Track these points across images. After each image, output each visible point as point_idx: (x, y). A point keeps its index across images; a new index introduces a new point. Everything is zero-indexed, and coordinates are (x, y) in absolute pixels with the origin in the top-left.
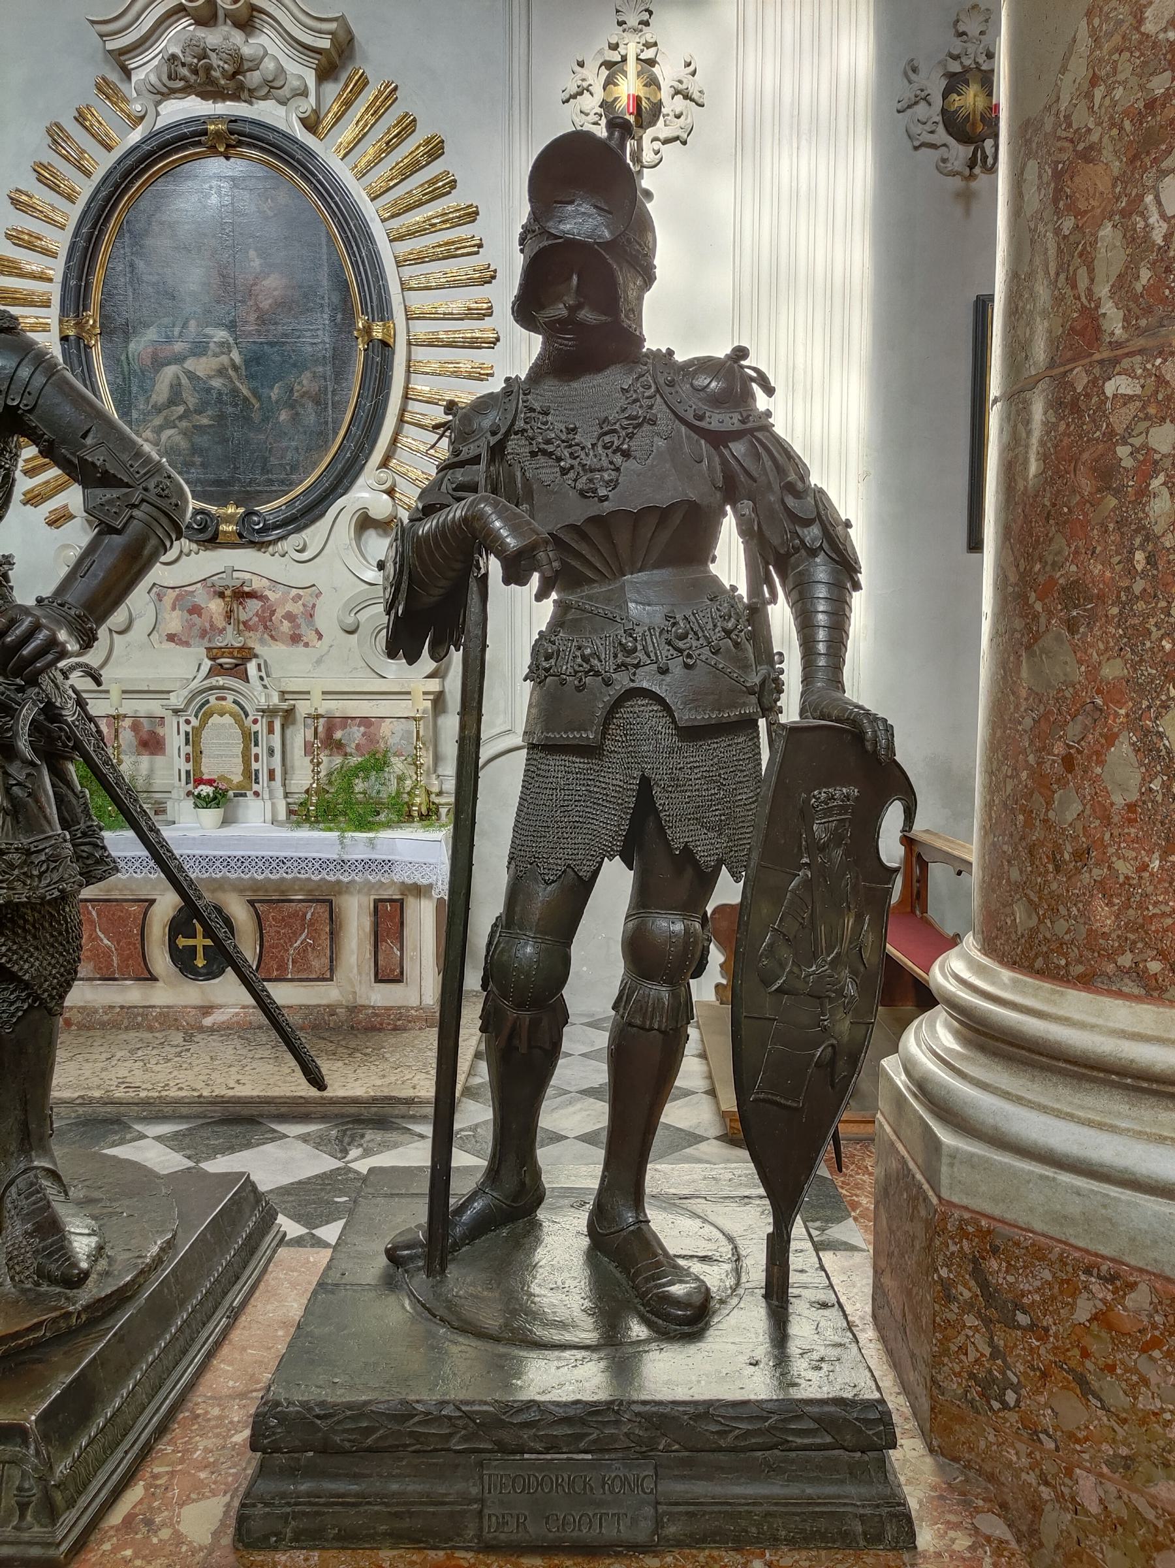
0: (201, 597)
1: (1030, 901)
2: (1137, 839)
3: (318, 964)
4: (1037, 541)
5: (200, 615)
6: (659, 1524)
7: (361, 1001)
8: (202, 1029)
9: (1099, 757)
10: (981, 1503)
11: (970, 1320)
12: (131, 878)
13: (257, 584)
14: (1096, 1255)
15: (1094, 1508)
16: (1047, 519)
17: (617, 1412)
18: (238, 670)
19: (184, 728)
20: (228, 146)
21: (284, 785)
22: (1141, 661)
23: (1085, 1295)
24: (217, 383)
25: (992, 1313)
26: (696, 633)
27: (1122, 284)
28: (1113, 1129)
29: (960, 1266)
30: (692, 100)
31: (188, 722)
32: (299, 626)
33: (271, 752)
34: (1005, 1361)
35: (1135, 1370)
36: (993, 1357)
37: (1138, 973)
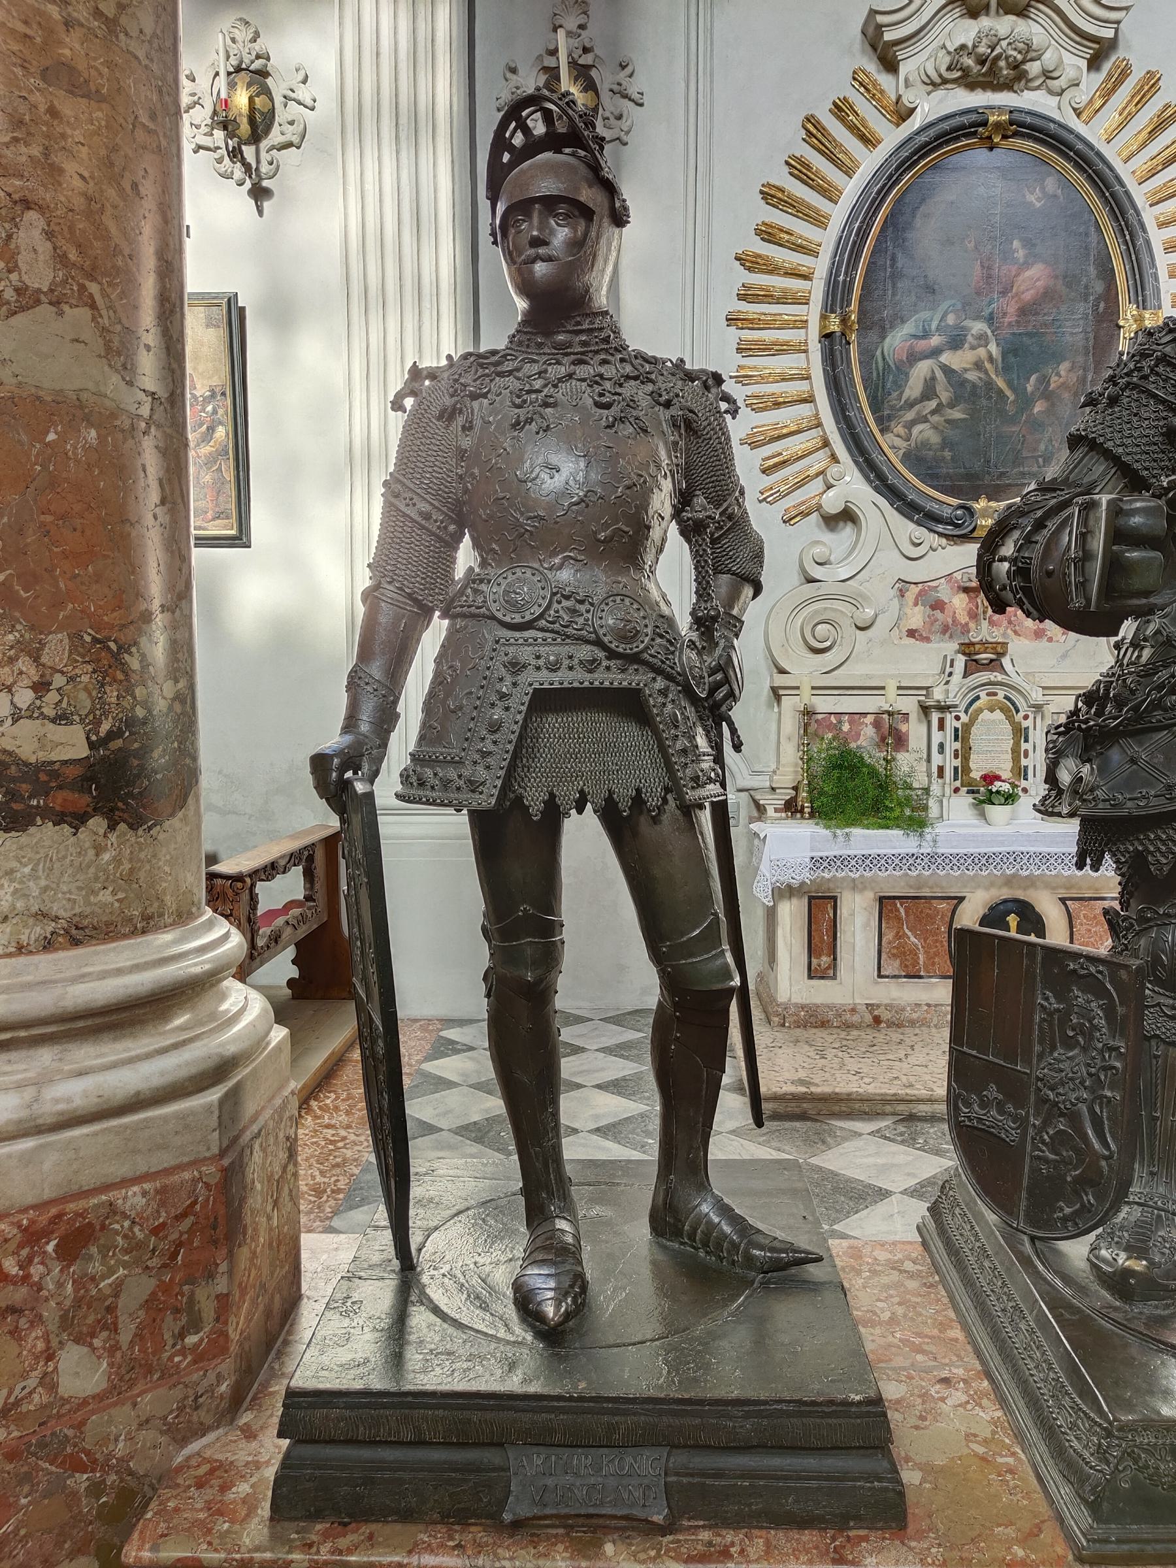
5: (942, 611)
12: (862, 876)
24: (972, 376)
31: (957, 718)
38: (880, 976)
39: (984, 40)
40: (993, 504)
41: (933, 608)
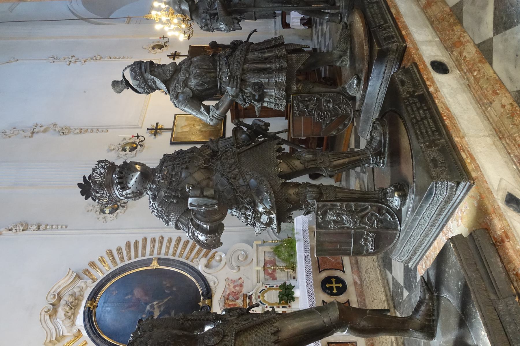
31: (267, 307)
32: (237, 285)
39: (65, 308)
40: (201, 300)
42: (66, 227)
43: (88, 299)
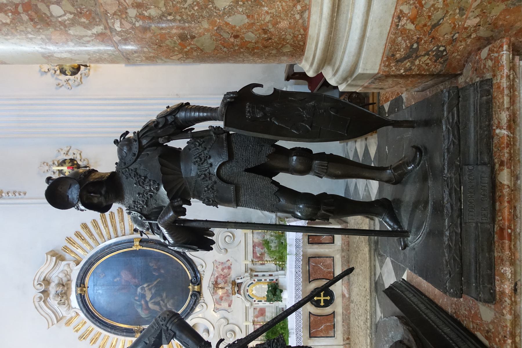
0: (217, 297)
1: (282, 47)
2: (258, 15)
3: (329, 261)
4: (168, 49)
5: (222, 297)
6: (484, 164)
7: (340, 248)
8: (349, 298)
9: (233, 27)
10: (477, 57)
11: (417, 62)
13: (213, 280)
14: (392, 23)
15: (478, 20)
16: (161, 46)
17: (447, 178)
18: (239, 285)
19: (256, 302)
20: (84, 287)
21: (274, 271)
22: (202, 16)
23: (405, 26)
24: (153, 291)
25: (414, 56)
26: (200, 155)
27: (86, 27)
28: (351, 19)
29: (400, 66)
30: (69, 150)
31: (255, 301)
32: (225, 267)
33: (264, 275)
34: (430, 51)
35: (430, 9)
36: (428, 55)
37: (302, 13)
38: (334, 337)
41: (222, 300)
42: (25, 194)
43: (77, 286)
